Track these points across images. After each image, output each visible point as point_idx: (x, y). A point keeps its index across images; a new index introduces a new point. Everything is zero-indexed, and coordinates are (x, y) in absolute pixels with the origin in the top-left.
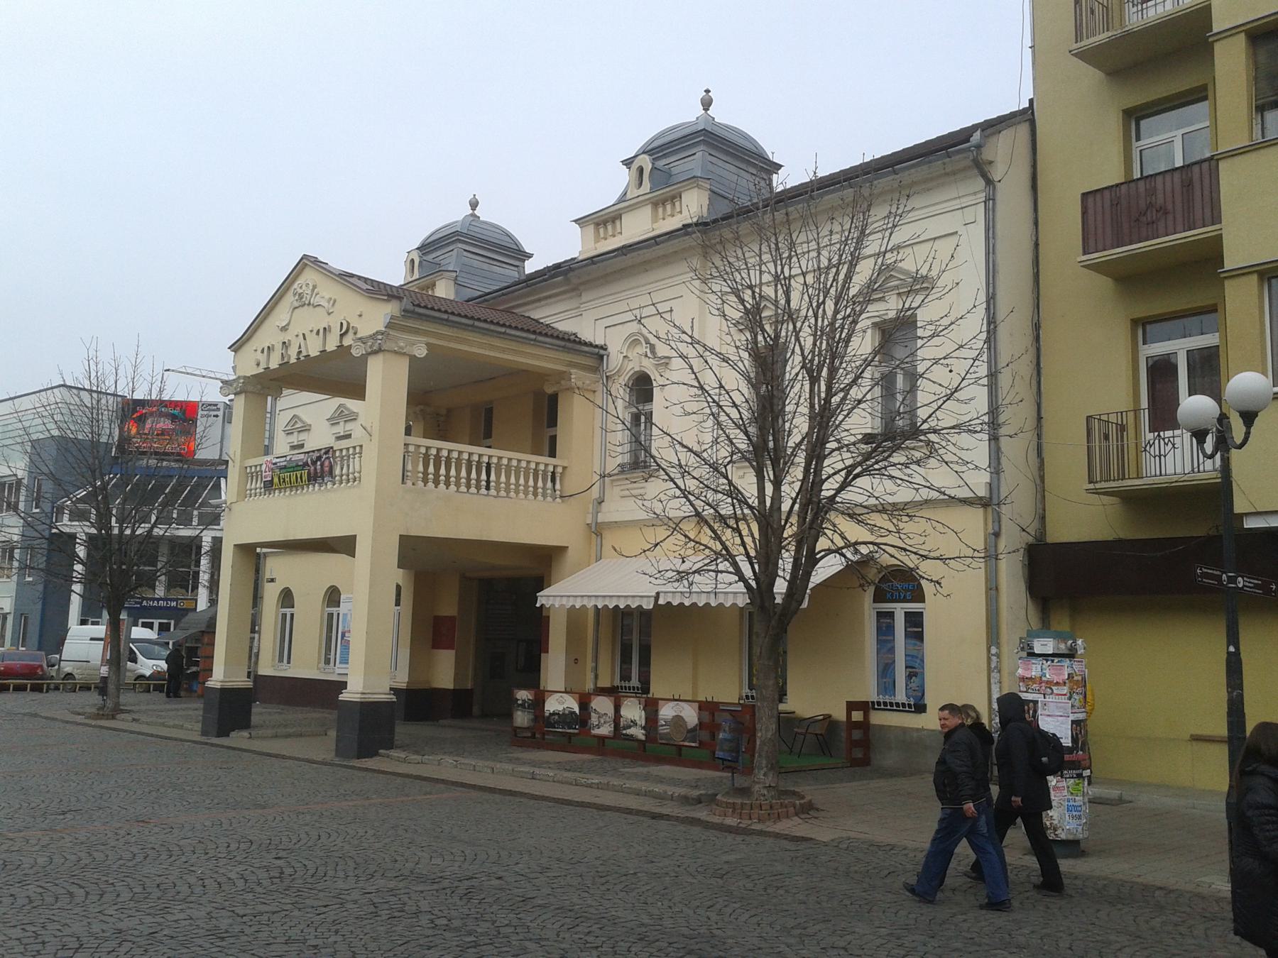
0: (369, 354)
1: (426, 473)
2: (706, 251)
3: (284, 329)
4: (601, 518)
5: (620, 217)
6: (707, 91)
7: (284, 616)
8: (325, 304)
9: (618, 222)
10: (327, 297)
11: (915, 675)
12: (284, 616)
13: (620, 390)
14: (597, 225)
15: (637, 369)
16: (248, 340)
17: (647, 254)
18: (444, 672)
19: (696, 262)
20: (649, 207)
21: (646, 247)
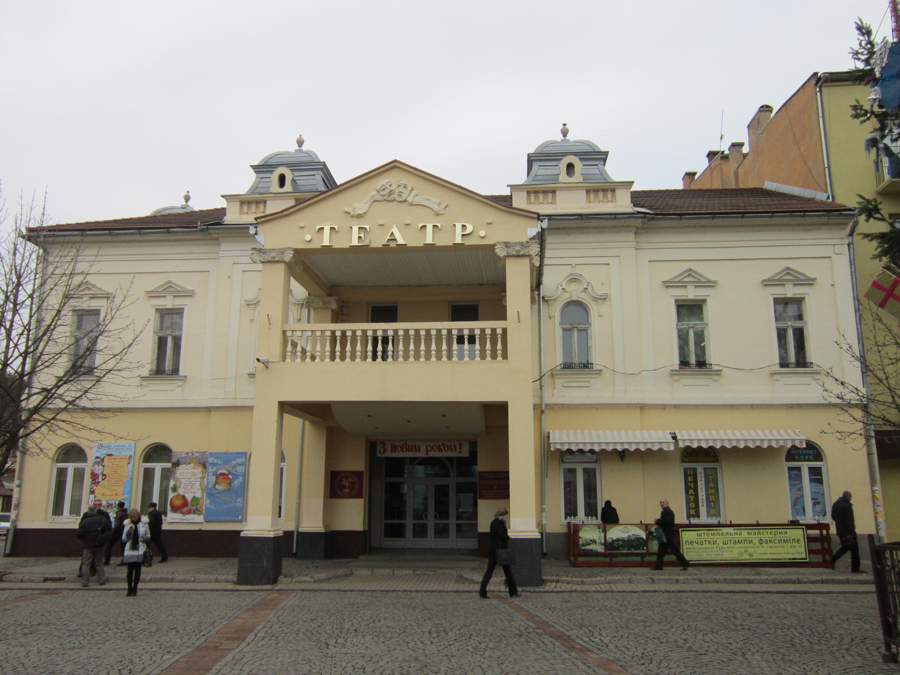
0: (513, 256)
1: (333, 353)
2: (638, 231)
3: (359, 216)
4: (548, 400)
5: (554, 192)
6: (564, 125)
7: (62, 473)
8: (436, 207)
9: (550, 196)
10: (438, 201)
11: (819, 503)
12: (62, 473)
13: (556, 310)
14: (529, 193)
15: (574, 298)
16: (286, 216)
17: (594, 223)
18: (352, 516)
19: (631, 237)
20: (583, 193)
21: (604, 219)
